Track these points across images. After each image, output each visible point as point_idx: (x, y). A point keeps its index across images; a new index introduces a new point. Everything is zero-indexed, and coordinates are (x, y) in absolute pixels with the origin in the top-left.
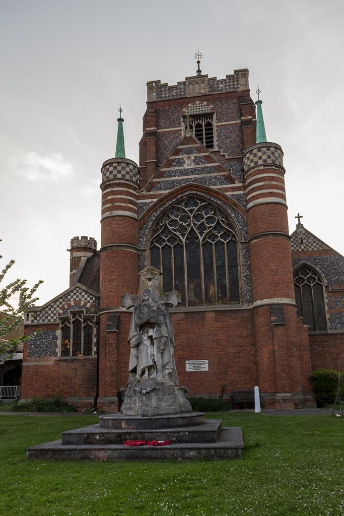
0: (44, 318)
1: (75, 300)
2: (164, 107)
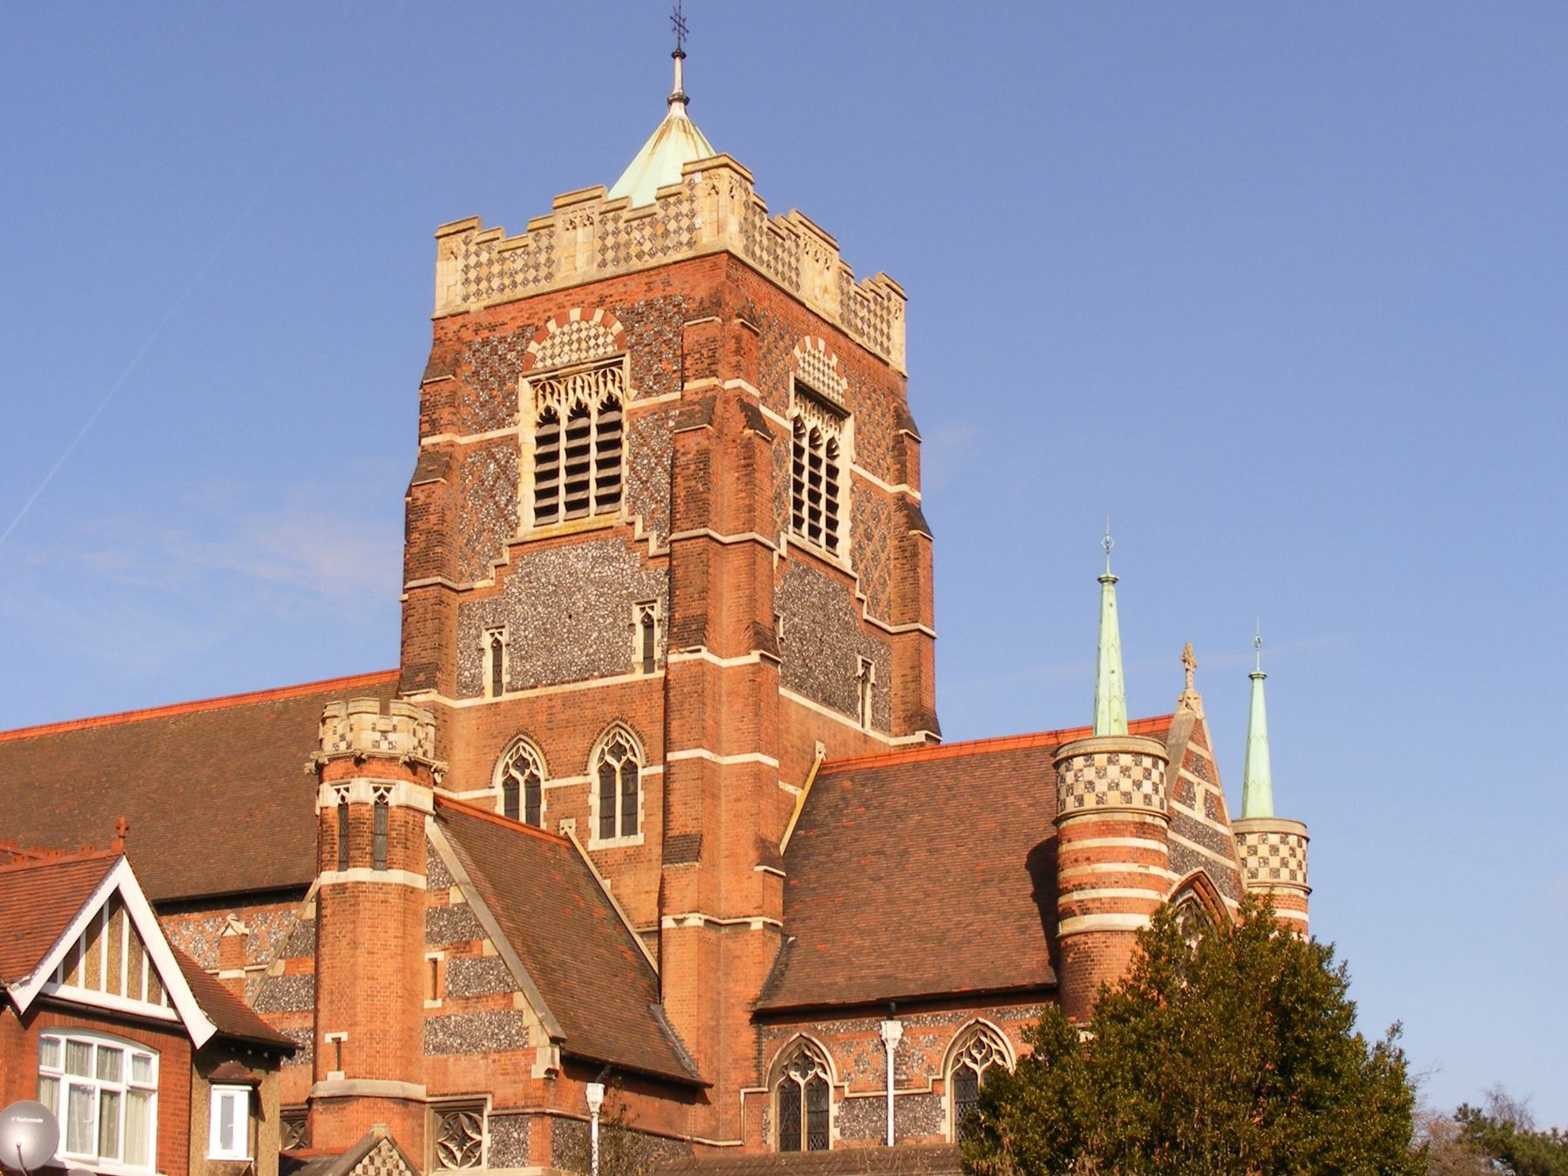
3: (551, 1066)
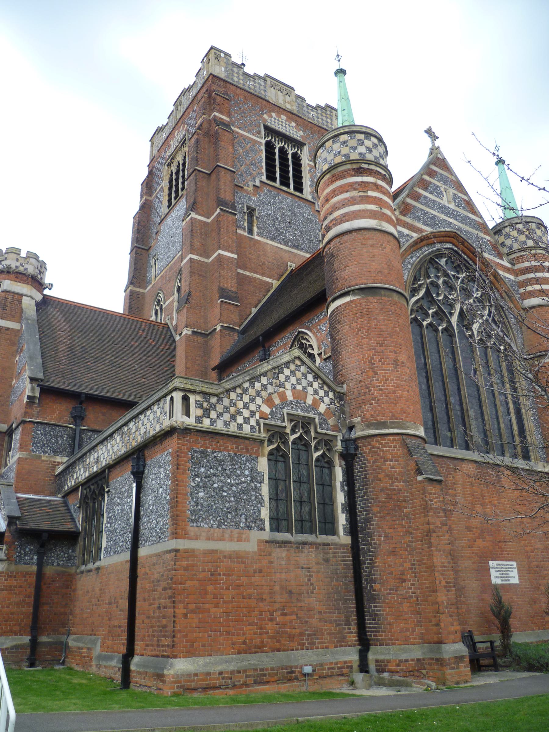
0: (227, 417)
1: (294, 388)
2: (238, 95)
3: (30, 394)
